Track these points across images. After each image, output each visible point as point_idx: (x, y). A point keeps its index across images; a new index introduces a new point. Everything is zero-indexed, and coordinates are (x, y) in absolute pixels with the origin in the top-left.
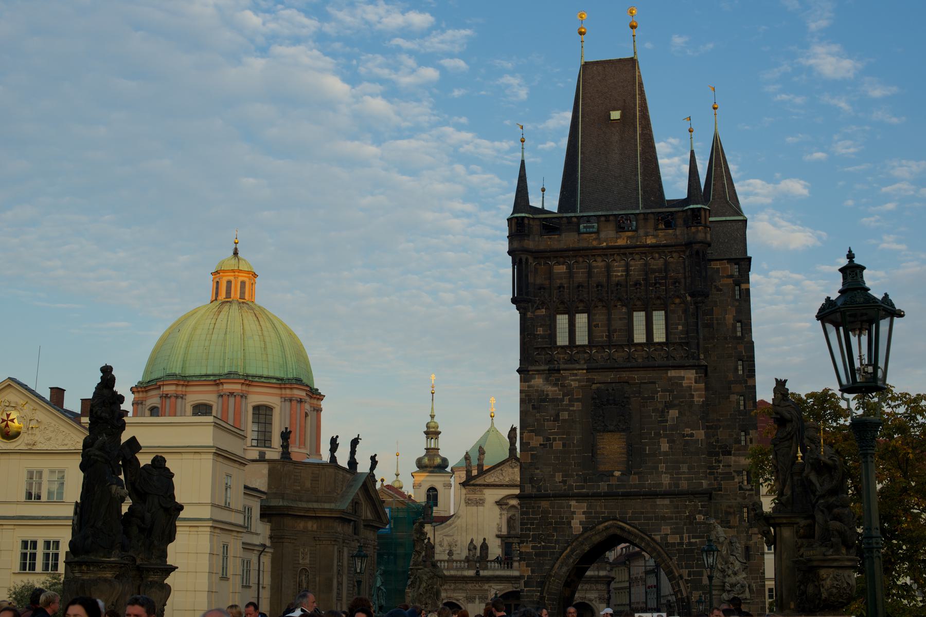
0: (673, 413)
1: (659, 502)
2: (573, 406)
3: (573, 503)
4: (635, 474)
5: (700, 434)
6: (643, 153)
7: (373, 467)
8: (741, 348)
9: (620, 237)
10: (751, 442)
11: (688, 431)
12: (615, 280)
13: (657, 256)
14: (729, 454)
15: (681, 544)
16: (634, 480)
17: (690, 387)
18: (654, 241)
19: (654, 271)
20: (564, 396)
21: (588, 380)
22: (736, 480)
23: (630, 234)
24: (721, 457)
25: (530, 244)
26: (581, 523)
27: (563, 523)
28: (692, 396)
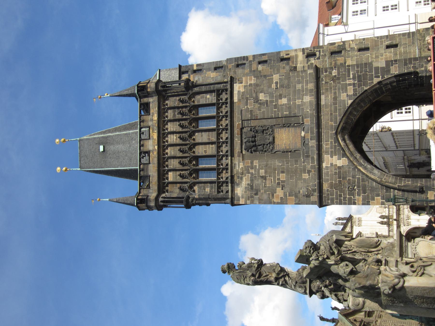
0: (262, 97)
1: (323, 102)
2: (256, 166)
3: (324, 165)
4: (303, 121)
6: (120, 131)
7: (338, 310)
8: (230, 66)
9: (153, 137)
10: (288, 54)
11: (274, 86)
12: (179, 141)
13: (166, 114)
14: (295, 68)
15: (354, 85)
16: (308, 122)
17: (245, 87)
19: (174, 115)
20: (249, 173)
21: (239, 156)
22: (313, 62)
23: (151, 131)
25: (153, 195)
26: (339, 159)
27: (340, 172)
28: (251, 85)
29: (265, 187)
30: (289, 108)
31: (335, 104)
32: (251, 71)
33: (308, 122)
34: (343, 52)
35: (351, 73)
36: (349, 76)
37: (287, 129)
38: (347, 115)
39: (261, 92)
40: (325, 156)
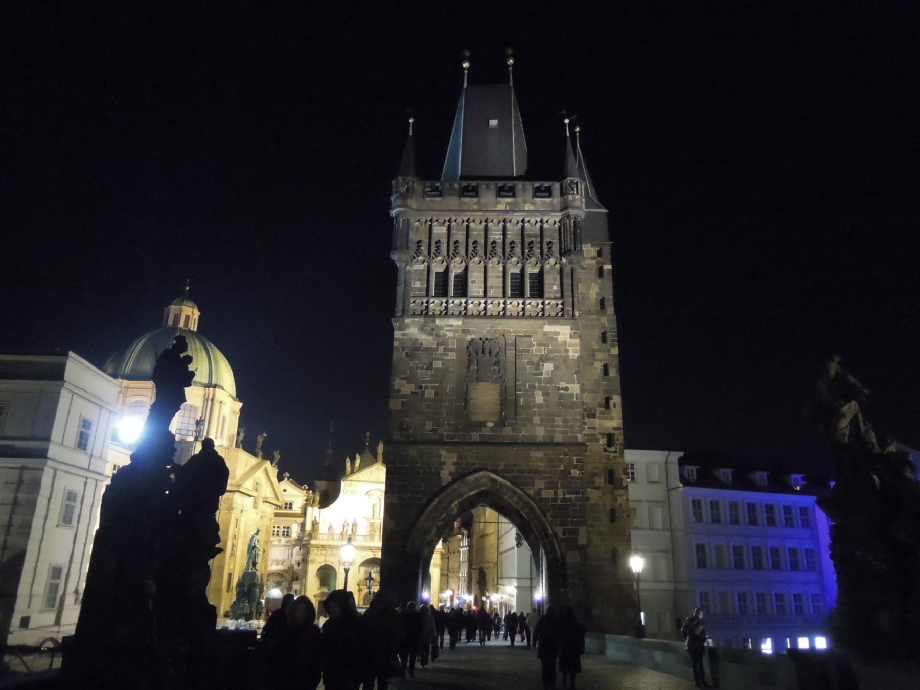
0: (548, 367)
2: (447, 355)
3: (443, 453)
5: (575, 388)
9: (499, 203)
10: (615, 406)
14: (594, 416)
15: (555, 499)
16: (508, 431)
17: (565, 343)
18: (532, 208)
19: (530, 236)
20: (438, 345)
22: (601, 442)
24: (586, 420)
26: (451, 474)
28: (567, 351)
29: (417, 368)
30: (527, 406)
31: (530, 471)
32: (595, 350)
33: (508, 431)
34: (611, 486)
35: (573, 496)
36: (569, 493)
37: (499, 402)
38: (513, 487)
39: (555, 367)
40: (456, 455)
